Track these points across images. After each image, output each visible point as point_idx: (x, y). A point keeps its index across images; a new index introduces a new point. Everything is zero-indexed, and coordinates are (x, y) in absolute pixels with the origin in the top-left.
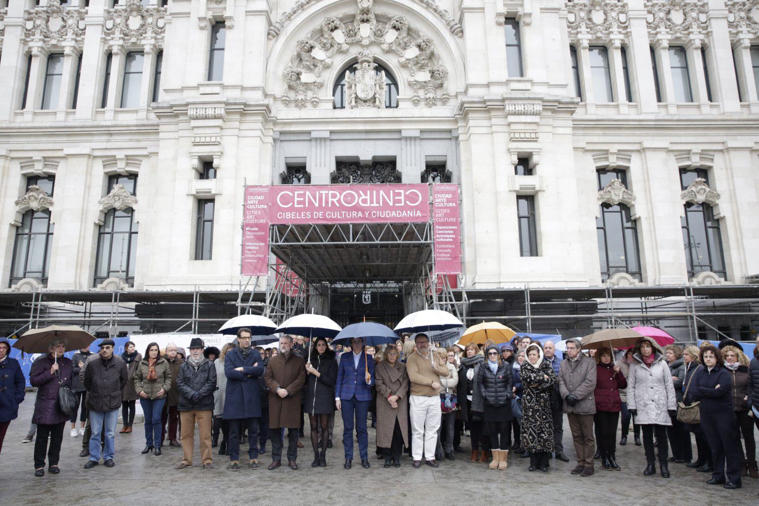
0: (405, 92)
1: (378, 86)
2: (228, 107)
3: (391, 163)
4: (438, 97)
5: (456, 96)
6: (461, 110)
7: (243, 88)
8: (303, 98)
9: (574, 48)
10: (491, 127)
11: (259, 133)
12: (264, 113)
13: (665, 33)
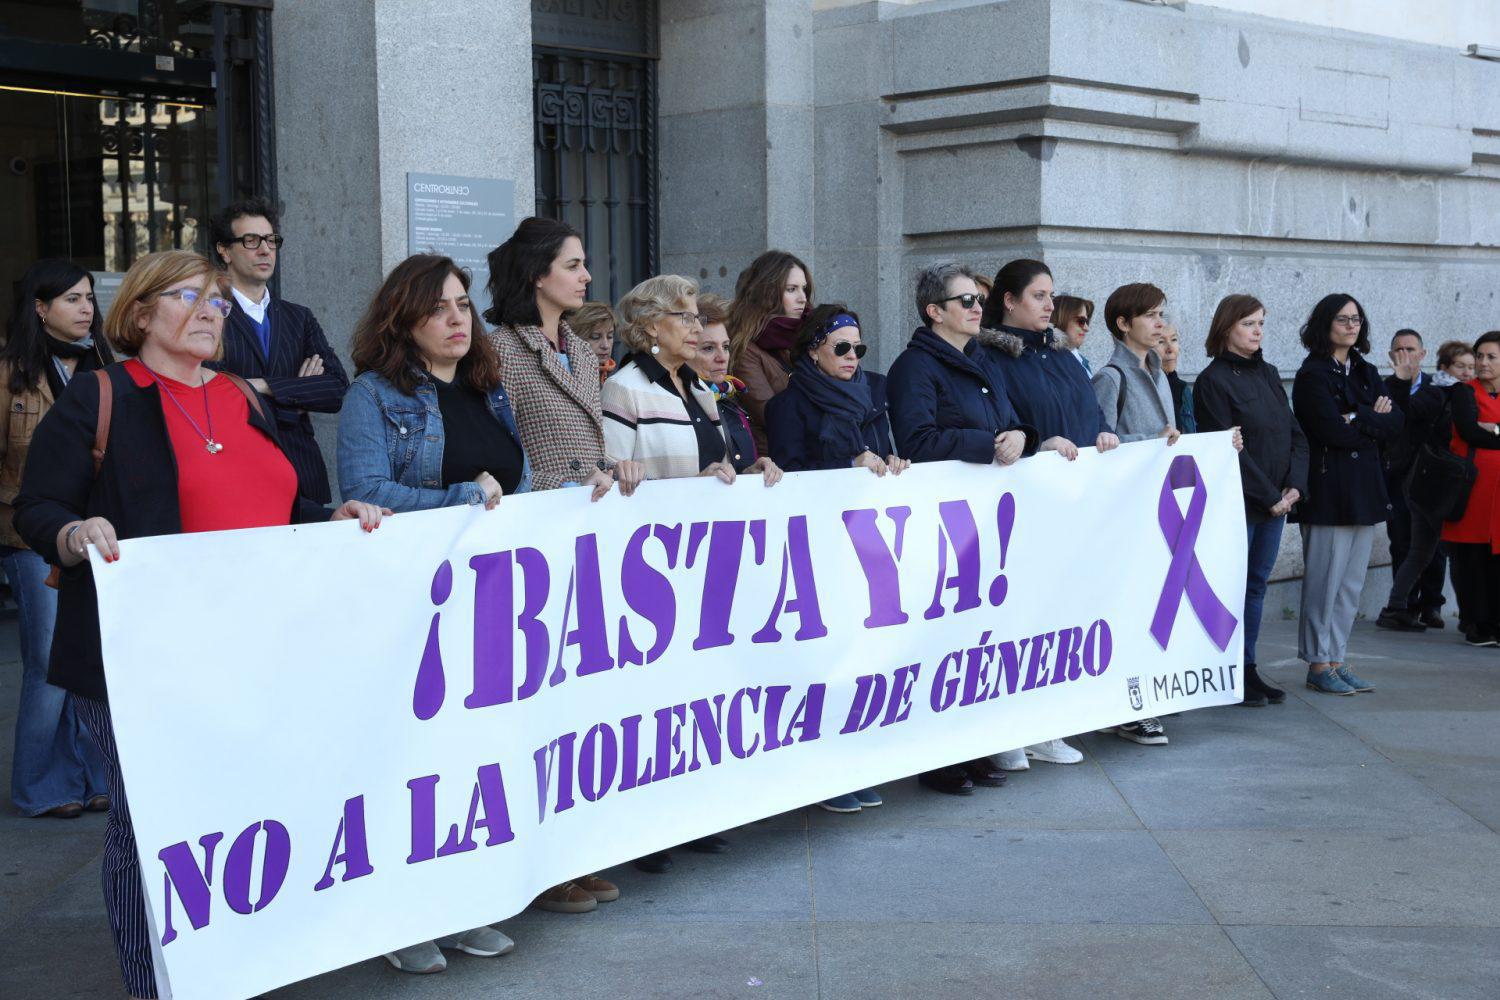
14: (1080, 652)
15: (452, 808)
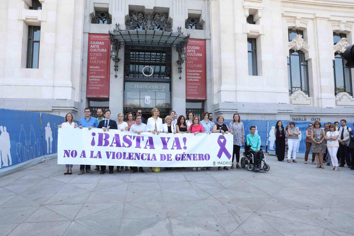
14: (204, 157)
15: (95, 154)
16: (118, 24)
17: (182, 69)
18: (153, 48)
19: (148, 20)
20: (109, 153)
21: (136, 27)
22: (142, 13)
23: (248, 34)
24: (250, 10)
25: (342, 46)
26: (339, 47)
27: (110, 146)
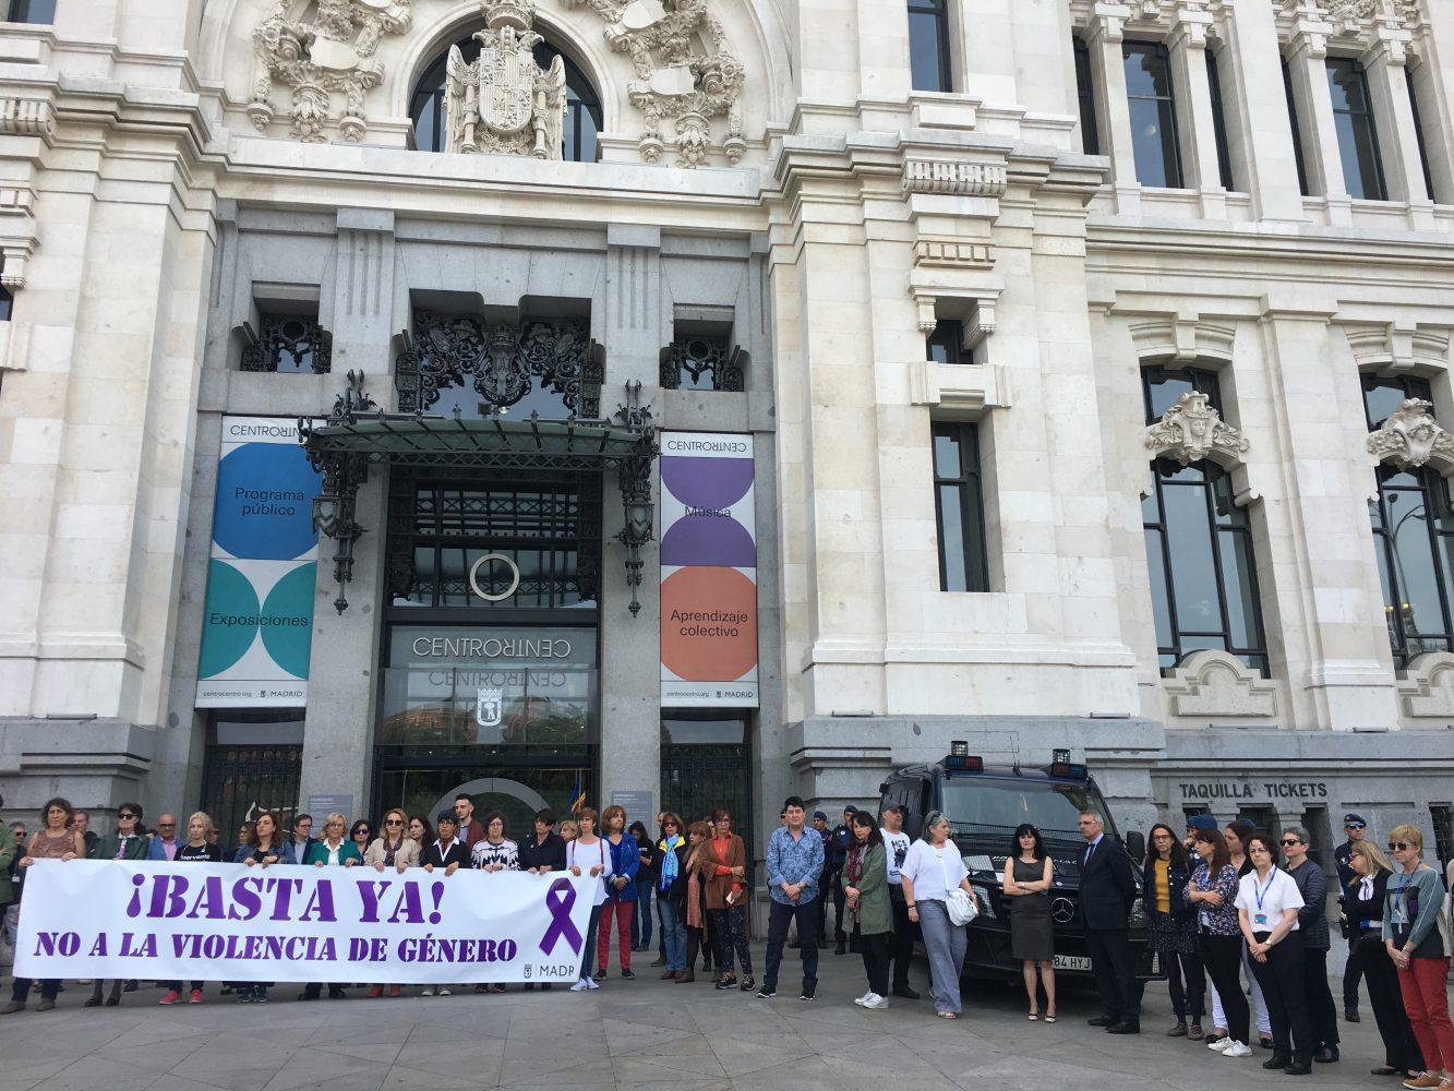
0: (619, 123)
1: (542, 97)
2: (63, 104)
3: (573, 317)
4: (714, 143)
5: (765, 142)
6: (778, 176)
7: (118, 56)
8: (317, 114)
9: (1083, 42)
10: (863, 225)
11: (164, 194)
12: (183, 135)
13: (1315, 17)
14: (496, 951)
15: (137, 943)
16: (357, 373)
17: (642, 571)
18: (521, 474)
19: (495, 349)
20: (183, 939)
21: (447, 379)
22: (472, 321)
23: (932, 407)
24: (941, 304)
25: (1408, 434)
26: (1397, 443)
27: (188, 916)
